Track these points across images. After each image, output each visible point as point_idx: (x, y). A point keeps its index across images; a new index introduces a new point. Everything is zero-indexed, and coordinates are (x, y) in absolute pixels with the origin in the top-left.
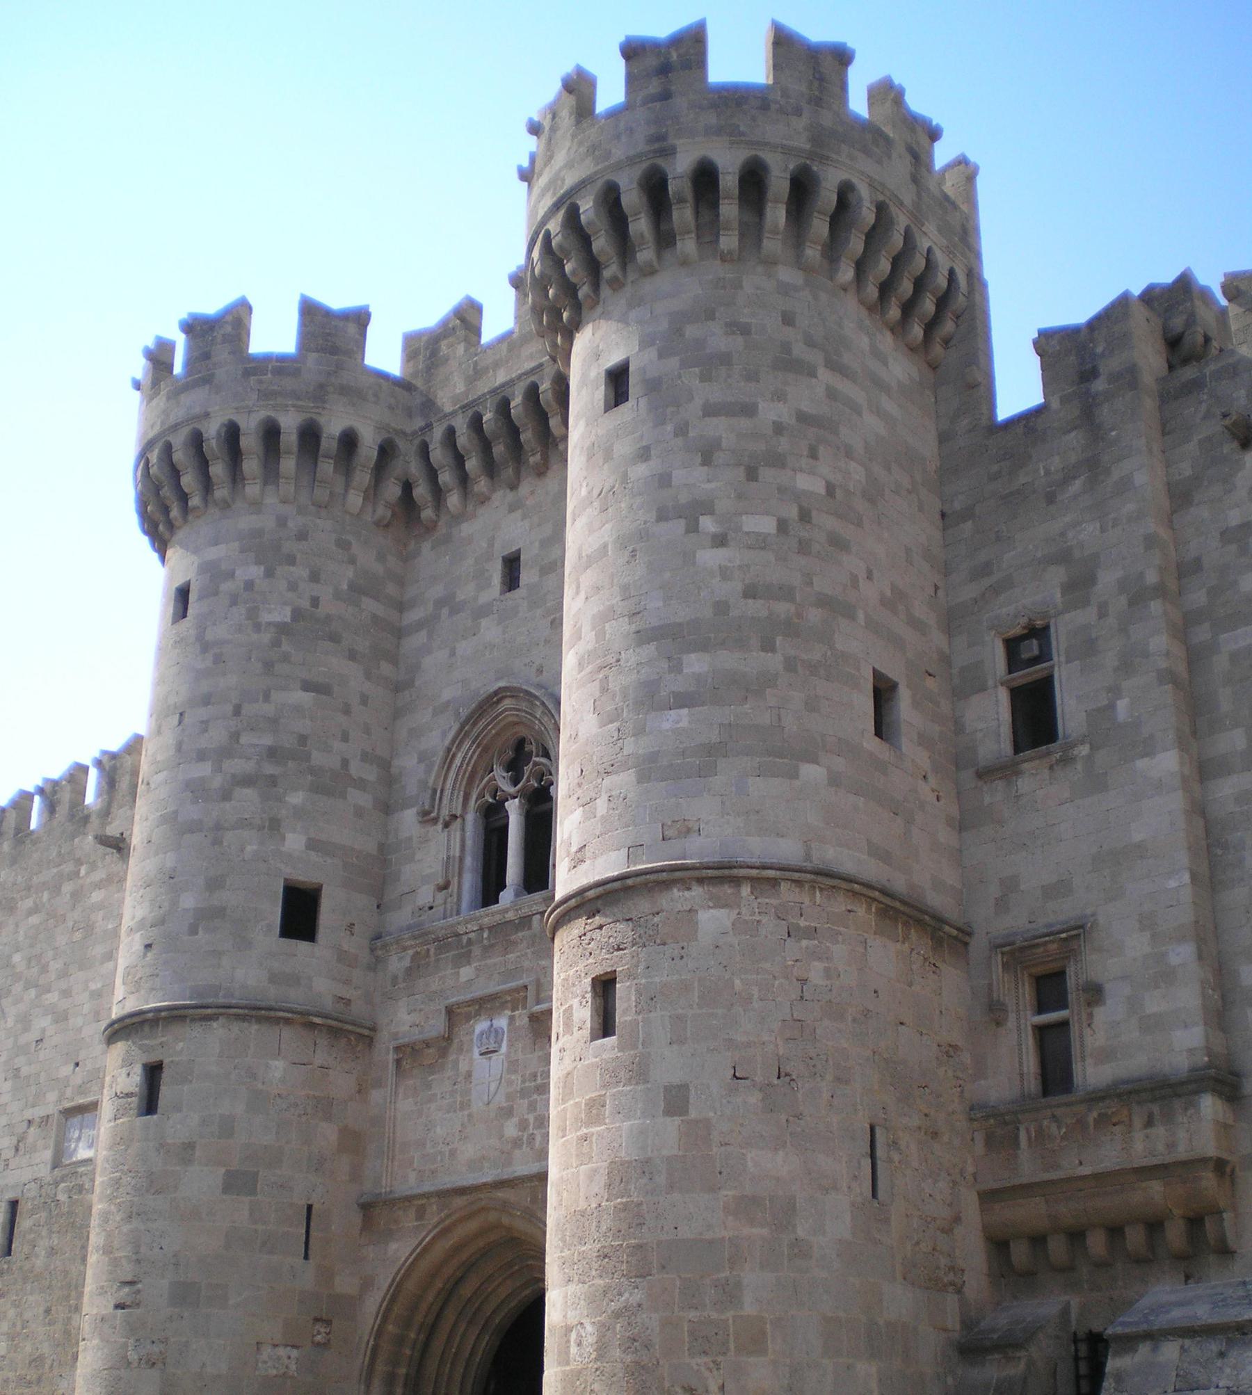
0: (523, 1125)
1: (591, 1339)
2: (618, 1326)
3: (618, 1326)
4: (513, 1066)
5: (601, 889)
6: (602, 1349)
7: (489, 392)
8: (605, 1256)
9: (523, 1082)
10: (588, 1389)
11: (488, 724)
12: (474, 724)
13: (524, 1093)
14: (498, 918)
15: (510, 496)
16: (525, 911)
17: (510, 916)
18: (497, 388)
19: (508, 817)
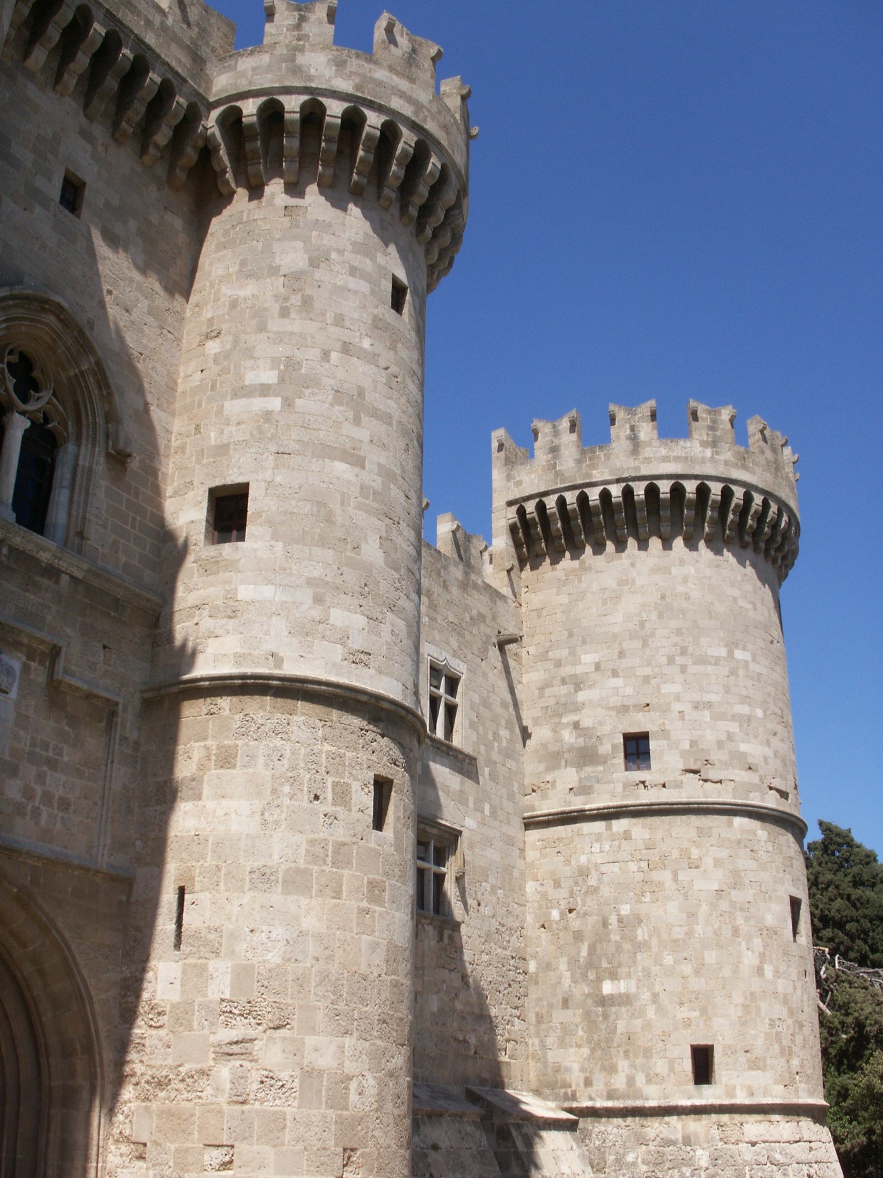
0: (29, 794)
1: (374, 1091)
2: (391, 1083)
3: (391, 1083)
4: (22, 720)
5: (393, 708)
6: (381, 1099)
7: (136, 36)
8: (384, 1022)
9: (33, 744)
10: (370, 1134)
11: (24, 319)
12: (16, 306)
13: (32, 758)
14: (30, 547)
15: (82, 119)
16: (63, 565)
17: (44, 556)
18: (144, 43)
19: (24, 437)
